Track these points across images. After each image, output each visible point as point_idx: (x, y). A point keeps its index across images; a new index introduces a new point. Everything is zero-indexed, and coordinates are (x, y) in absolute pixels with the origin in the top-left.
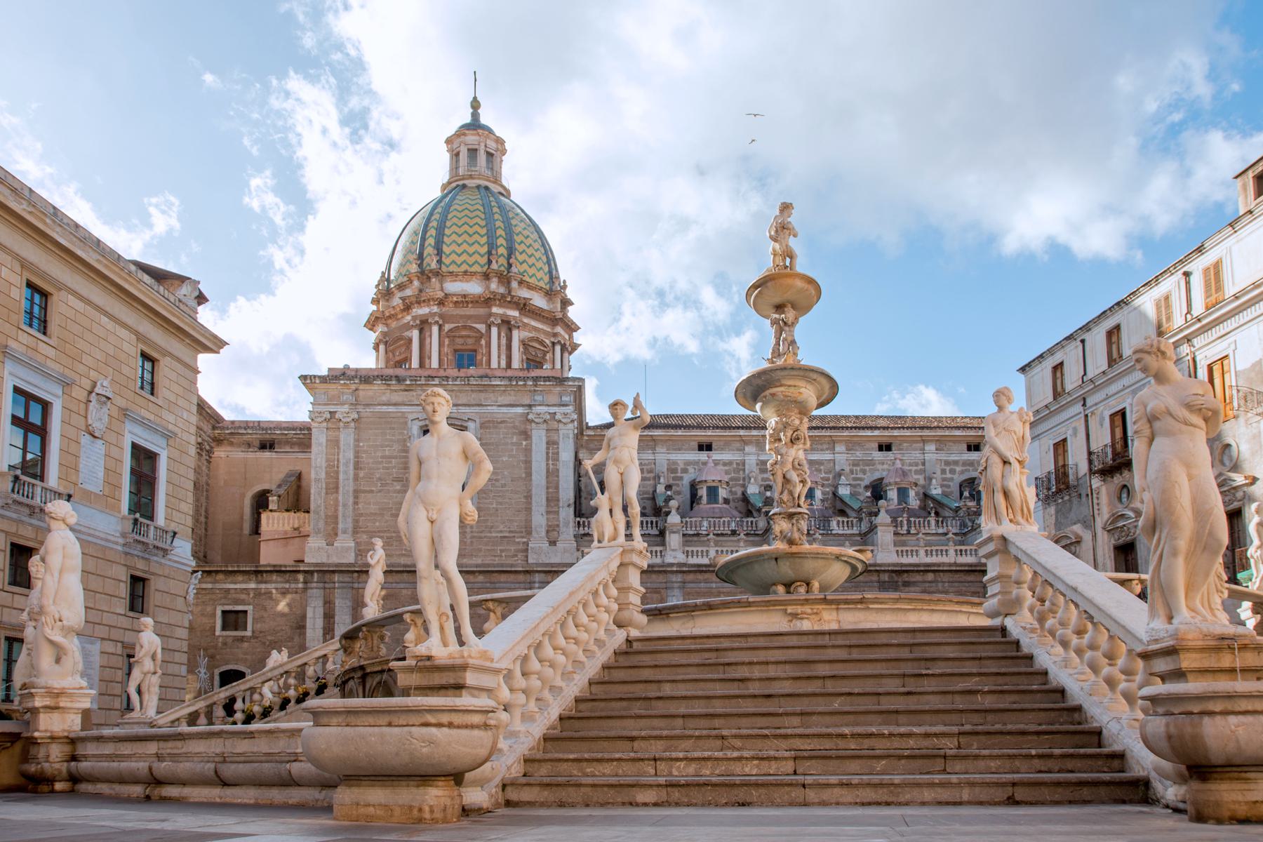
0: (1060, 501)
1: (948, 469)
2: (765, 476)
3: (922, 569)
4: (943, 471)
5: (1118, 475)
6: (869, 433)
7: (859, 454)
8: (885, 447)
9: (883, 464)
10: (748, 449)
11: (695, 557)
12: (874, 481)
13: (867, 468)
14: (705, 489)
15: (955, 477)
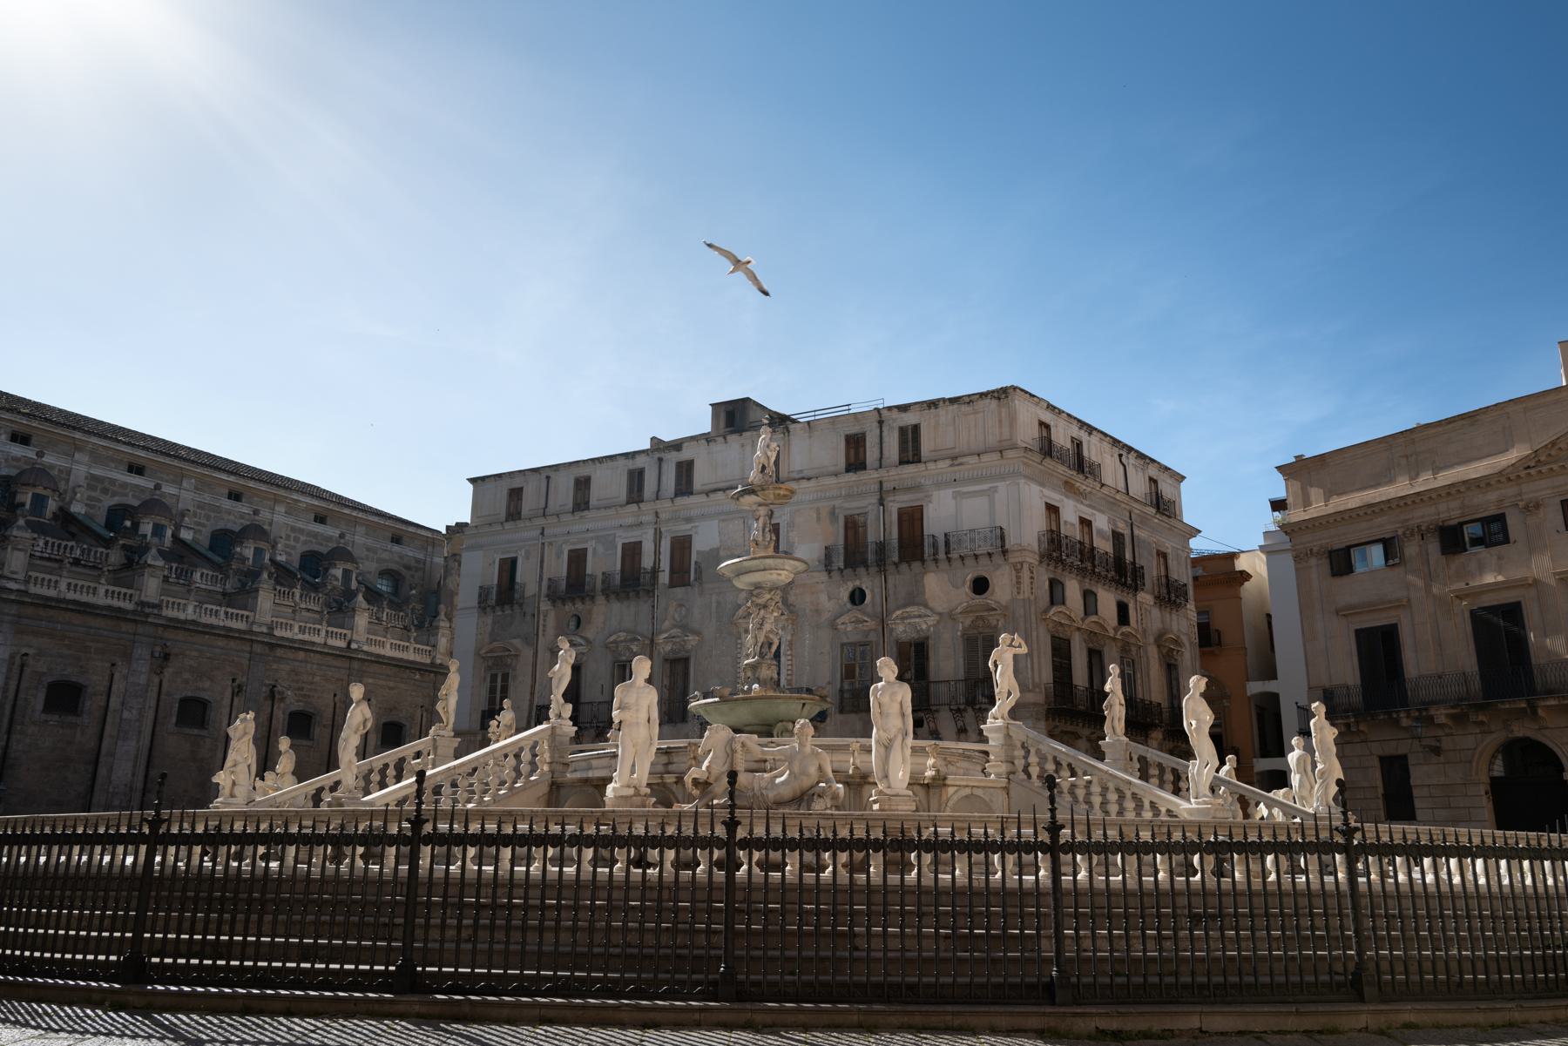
0: (500, 613)
1: (293, 535)
2: (93, 494)
3: (296, 645)
4: (288, 537)
5: (570, 604)
6: (224, 477)
7: (207, 498)
8: (235, 496)
9: (230, 513)
10: (77, 456)
11: (39, 586)
12: (217, 531)
13: (213, 514)
14: (30, 495)
15: (298, 545)
